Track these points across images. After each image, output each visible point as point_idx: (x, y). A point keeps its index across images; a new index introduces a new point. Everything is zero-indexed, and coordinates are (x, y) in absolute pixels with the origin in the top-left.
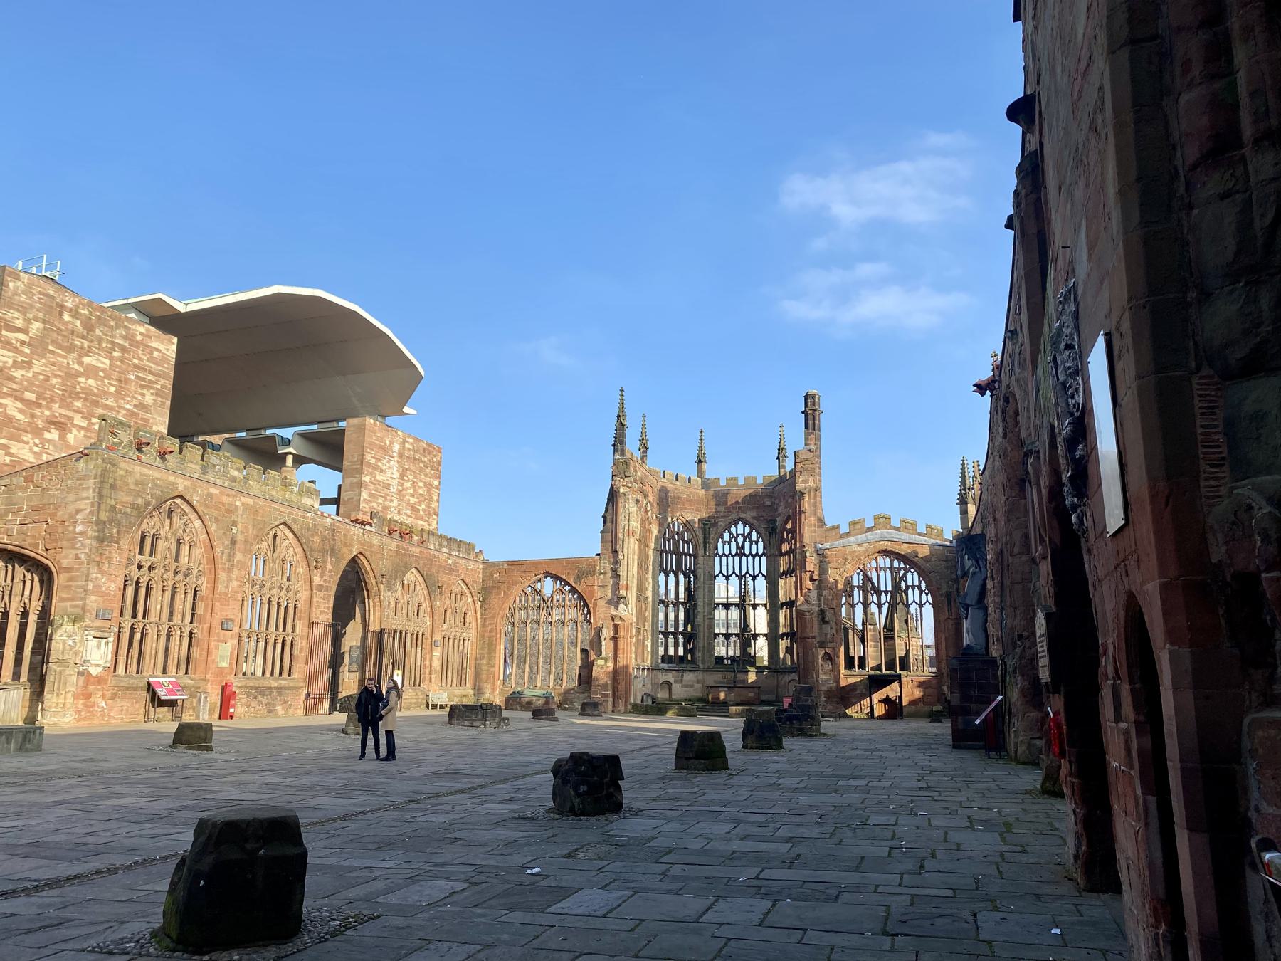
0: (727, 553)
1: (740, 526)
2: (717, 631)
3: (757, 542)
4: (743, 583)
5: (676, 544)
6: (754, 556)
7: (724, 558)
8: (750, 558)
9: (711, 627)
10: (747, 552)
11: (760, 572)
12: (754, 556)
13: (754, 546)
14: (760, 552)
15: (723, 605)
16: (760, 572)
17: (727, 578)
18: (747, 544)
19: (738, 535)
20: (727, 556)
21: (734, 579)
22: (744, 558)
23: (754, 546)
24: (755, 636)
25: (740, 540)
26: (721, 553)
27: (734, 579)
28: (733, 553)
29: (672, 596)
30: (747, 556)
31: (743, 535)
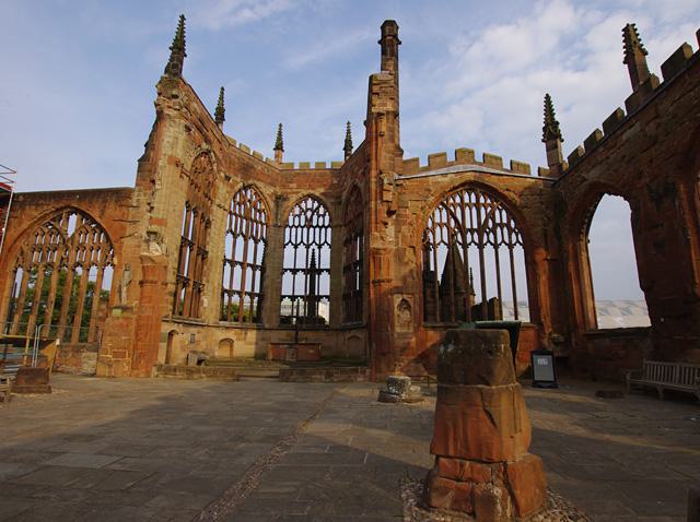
0: (296, 224)
1: (310, 201)
2: (283, 294)
3: (324, 216)
4: (310, 254)
5: (248, 211)
6: (321, 228)
7: (294, 229)
8: (317, 229)
9: (280, 289)
10: (315, 224)
11: (326, 241)
12: (321, 228)
13: (321, 218)
14: (326, 224)
15: (291, 270)
16: (326, 241)
17: (296, 246)
18: (315, 217)
19: (307, 210)
20: (297, 227)
21: (302, 248)
22: (312, 229)
23: (321, 218)
24: (319, 298)
25: (309, 214)
26: (291, 224)
27: (302, 248)
28: (302, 224)
29: (239, 258)
30: (315, 228)
31: (311, 209)
